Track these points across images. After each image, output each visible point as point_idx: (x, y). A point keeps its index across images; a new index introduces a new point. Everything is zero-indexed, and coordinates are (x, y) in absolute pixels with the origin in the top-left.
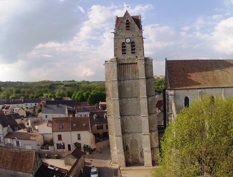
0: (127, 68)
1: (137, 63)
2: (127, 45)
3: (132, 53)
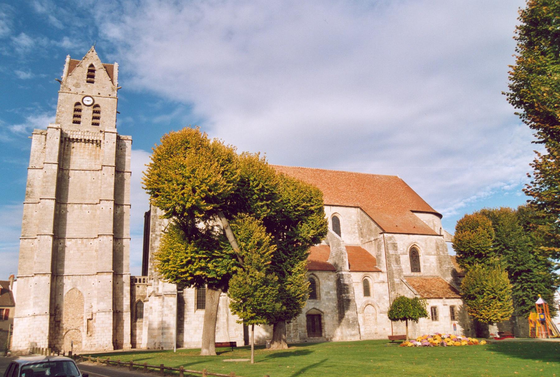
2: (83, 107)
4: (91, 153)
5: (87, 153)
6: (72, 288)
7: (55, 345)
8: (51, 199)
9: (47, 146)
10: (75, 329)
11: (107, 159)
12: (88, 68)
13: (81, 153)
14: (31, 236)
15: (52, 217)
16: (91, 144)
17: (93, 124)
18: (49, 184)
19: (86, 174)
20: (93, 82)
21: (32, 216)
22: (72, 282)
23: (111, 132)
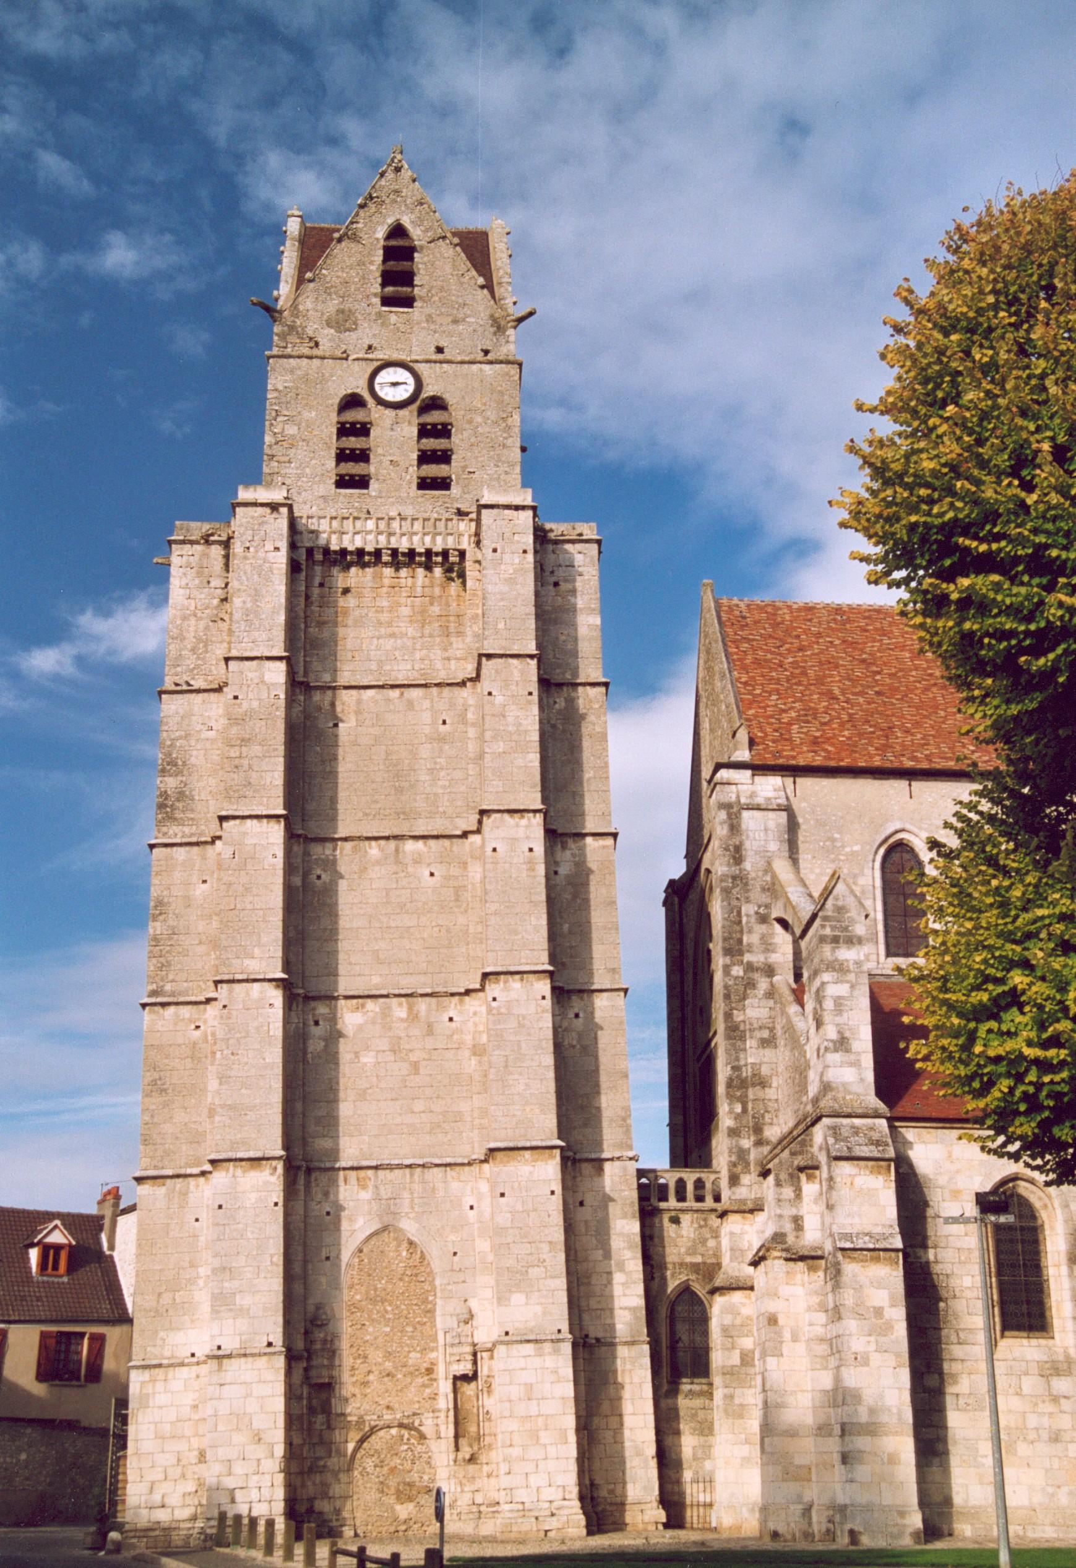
2: (375, 413)
4: (423, 612)
5: (405, 611)
6: (375, 1226)
7: (311, 1500)
8: (269, 817)
9: (234, 584)
10: (401, 1426)
11: (501, 626)
12: (382, 243)
13: (380, 610)
14: (185, 993)
15: (275, 898)
16: (420, 571)
17: (425, 484)
18: (256, 750)
19: (410, 705)
20: (408, 302)
21: (188, 901)
22: (378, 1198)
23: (508, 507)
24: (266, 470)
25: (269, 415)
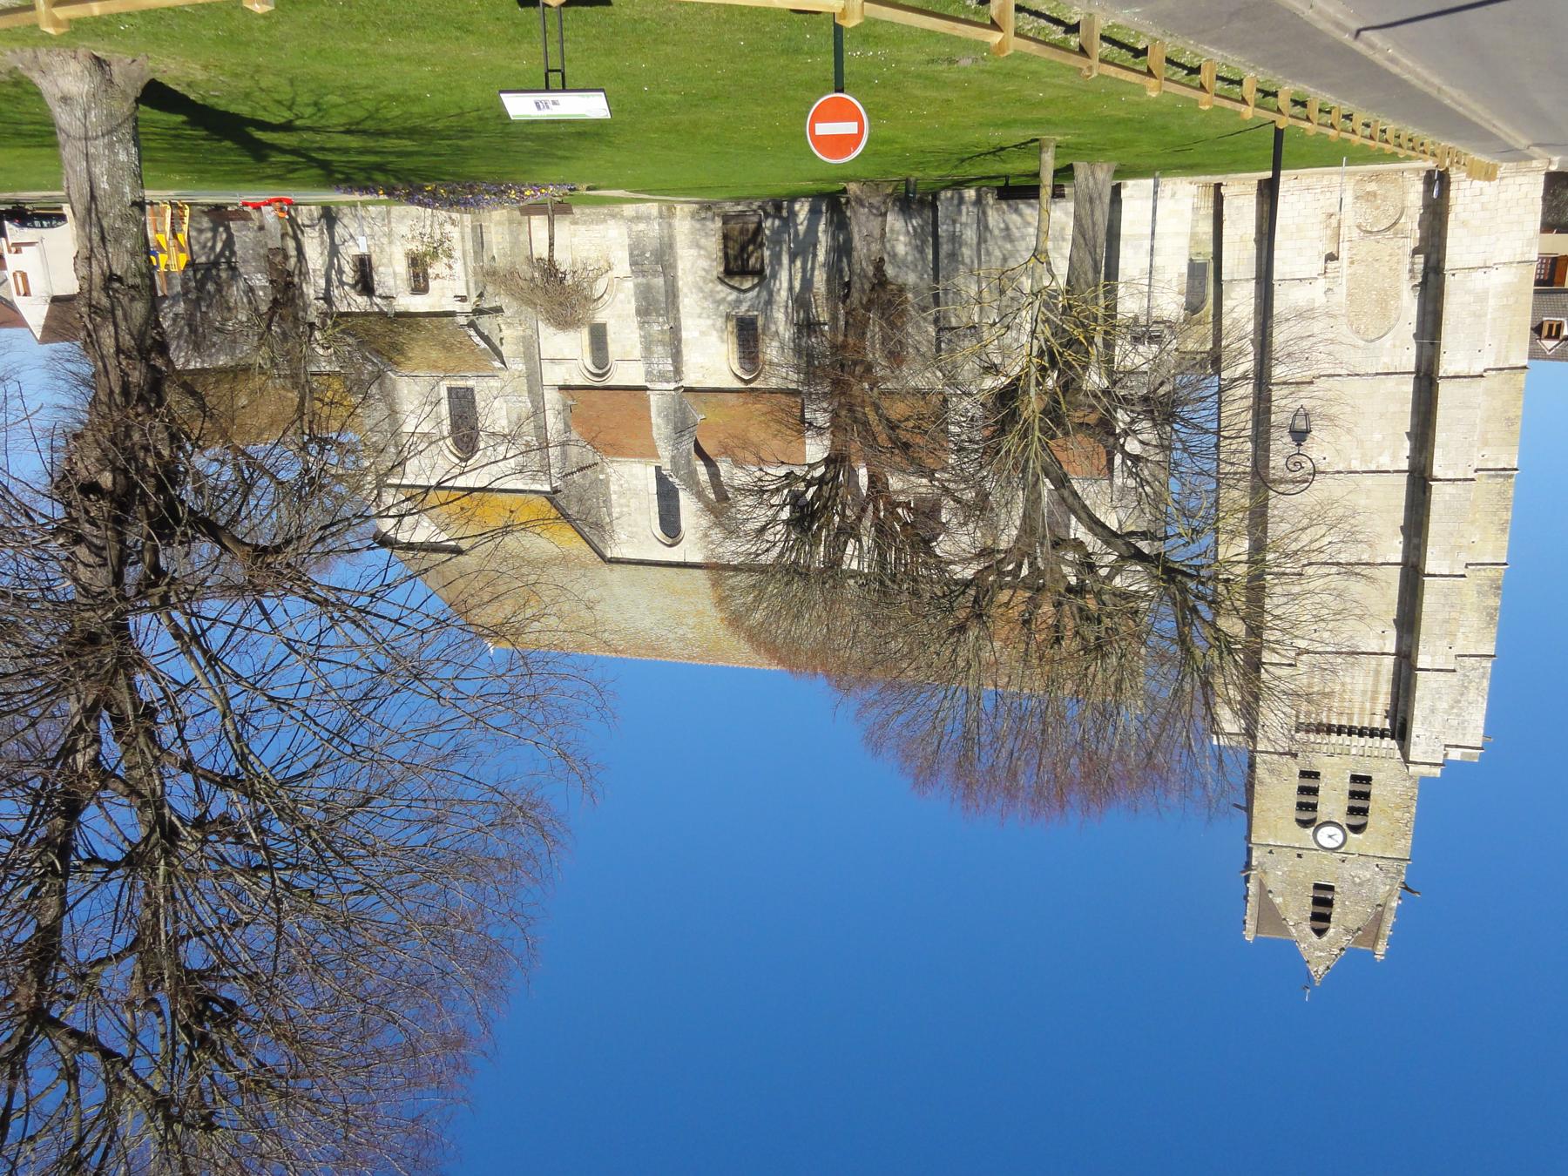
0: (1356, 710)
1: (1297, 731)
2: (1342, 817)
3: (1316, 775)
10: (1371, 232)
12: (1332, 925)
20: (1317, 887)
24: (1416, 791)
25: (1411, 825)
